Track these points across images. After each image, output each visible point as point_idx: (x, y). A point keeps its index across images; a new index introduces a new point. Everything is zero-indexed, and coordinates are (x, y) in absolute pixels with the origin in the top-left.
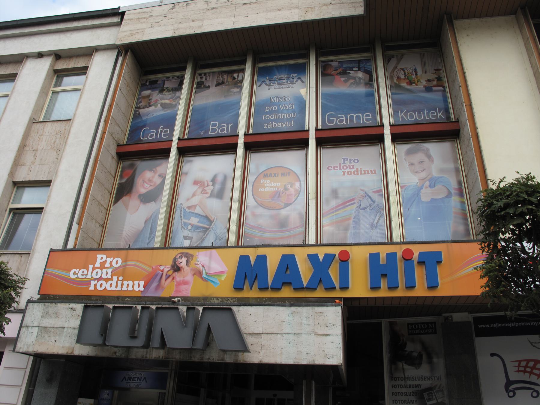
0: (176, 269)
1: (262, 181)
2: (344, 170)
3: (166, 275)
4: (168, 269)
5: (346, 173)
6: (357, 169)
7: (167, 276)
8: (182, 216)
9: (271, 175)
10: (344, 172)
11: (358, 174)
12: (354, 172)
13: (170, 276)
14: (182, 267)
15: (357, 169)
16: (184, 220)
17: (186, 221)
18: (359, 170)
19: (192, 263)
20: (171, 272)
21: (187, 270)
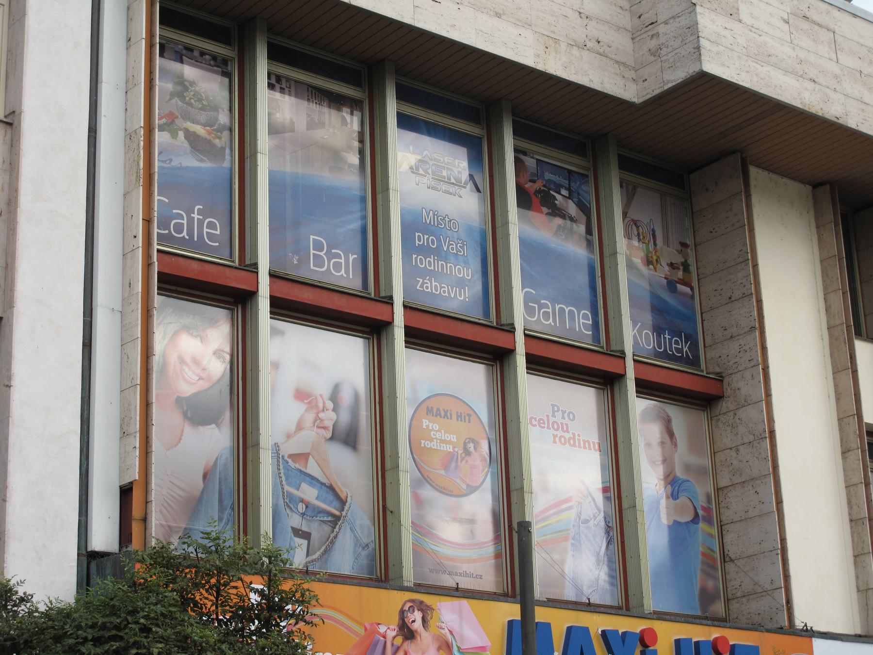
0: (407, 633)
1: (425, 423)
2: (556, 433)
3: (393, 645)
4: (394, 633)
5: (557, 439)
6: (574, 434)
7: (395, 648)
8: (283, 478)
9: (438, 414)
10: (555, 436)
11: (574, 445)
12: (570, 438)
13: (398, 648)
14: (416, 631)
15: (574, 434)
16: (287, 488)
17: (292, 490)
18: (577, 437)
19: (432, 623)
20: (399, 640)
21: (425, 637)
